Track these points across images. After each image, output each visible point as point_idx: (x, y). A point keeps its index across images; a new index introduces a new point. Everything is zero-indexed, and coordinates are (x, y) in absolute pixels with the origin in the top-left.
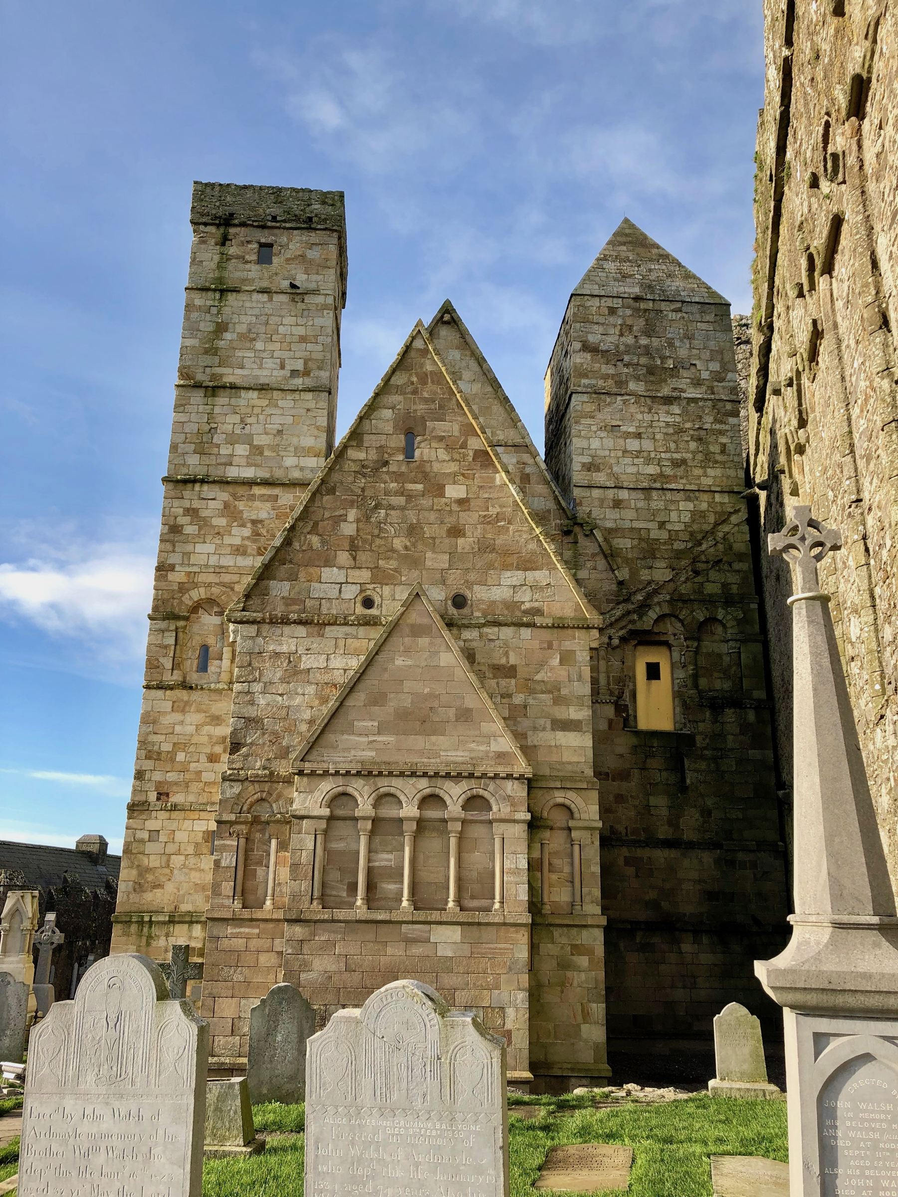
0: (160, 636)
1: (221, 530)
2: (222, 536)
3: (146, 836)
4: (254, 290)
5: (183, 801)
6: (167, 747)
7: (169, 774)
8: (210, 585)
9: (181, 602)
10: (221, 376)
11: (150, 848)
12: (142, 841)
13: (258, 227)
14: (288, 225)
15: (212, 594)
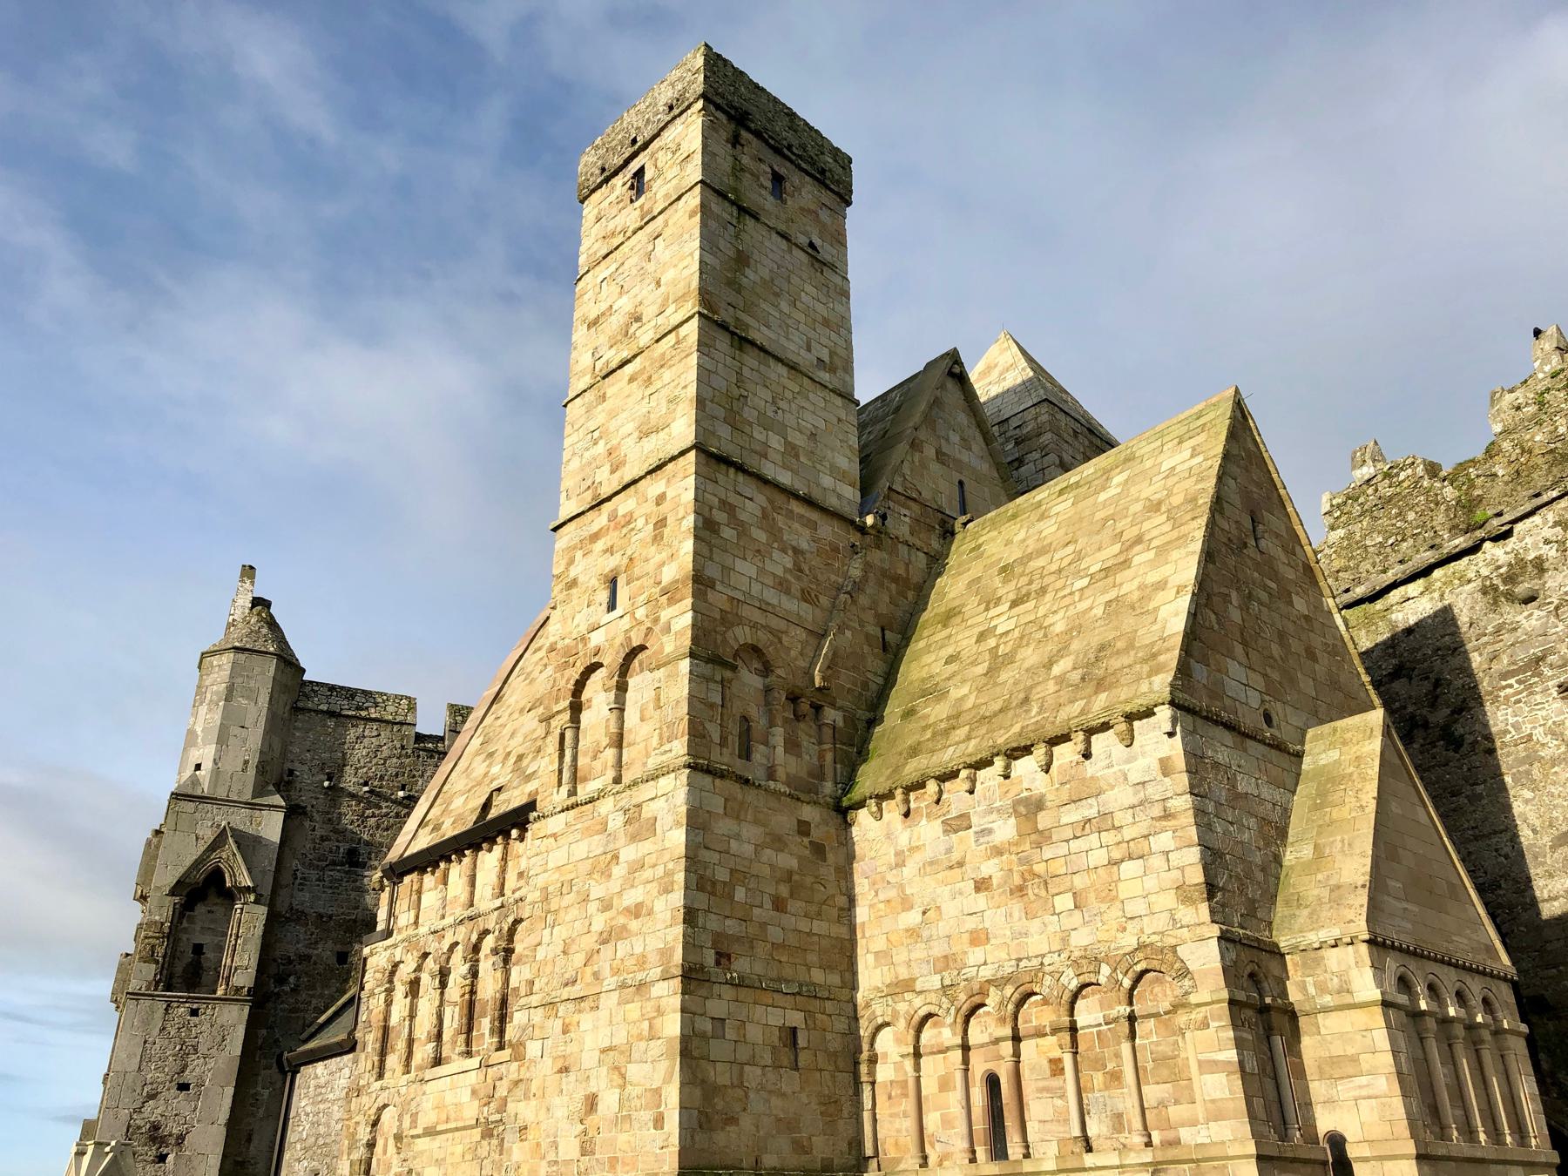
0: (704, 686)
1: (762, 548)
2: (764, 557)
4: (773, 228)
5: (748, 971)
6: (722, 875)
7: (728, 922)
9: (725, 640)
10: (747, 326)
11: (717, 1049)
12: (703, 1036)
13: (771, 147)
14: (804, 165)
15: (758, 640)
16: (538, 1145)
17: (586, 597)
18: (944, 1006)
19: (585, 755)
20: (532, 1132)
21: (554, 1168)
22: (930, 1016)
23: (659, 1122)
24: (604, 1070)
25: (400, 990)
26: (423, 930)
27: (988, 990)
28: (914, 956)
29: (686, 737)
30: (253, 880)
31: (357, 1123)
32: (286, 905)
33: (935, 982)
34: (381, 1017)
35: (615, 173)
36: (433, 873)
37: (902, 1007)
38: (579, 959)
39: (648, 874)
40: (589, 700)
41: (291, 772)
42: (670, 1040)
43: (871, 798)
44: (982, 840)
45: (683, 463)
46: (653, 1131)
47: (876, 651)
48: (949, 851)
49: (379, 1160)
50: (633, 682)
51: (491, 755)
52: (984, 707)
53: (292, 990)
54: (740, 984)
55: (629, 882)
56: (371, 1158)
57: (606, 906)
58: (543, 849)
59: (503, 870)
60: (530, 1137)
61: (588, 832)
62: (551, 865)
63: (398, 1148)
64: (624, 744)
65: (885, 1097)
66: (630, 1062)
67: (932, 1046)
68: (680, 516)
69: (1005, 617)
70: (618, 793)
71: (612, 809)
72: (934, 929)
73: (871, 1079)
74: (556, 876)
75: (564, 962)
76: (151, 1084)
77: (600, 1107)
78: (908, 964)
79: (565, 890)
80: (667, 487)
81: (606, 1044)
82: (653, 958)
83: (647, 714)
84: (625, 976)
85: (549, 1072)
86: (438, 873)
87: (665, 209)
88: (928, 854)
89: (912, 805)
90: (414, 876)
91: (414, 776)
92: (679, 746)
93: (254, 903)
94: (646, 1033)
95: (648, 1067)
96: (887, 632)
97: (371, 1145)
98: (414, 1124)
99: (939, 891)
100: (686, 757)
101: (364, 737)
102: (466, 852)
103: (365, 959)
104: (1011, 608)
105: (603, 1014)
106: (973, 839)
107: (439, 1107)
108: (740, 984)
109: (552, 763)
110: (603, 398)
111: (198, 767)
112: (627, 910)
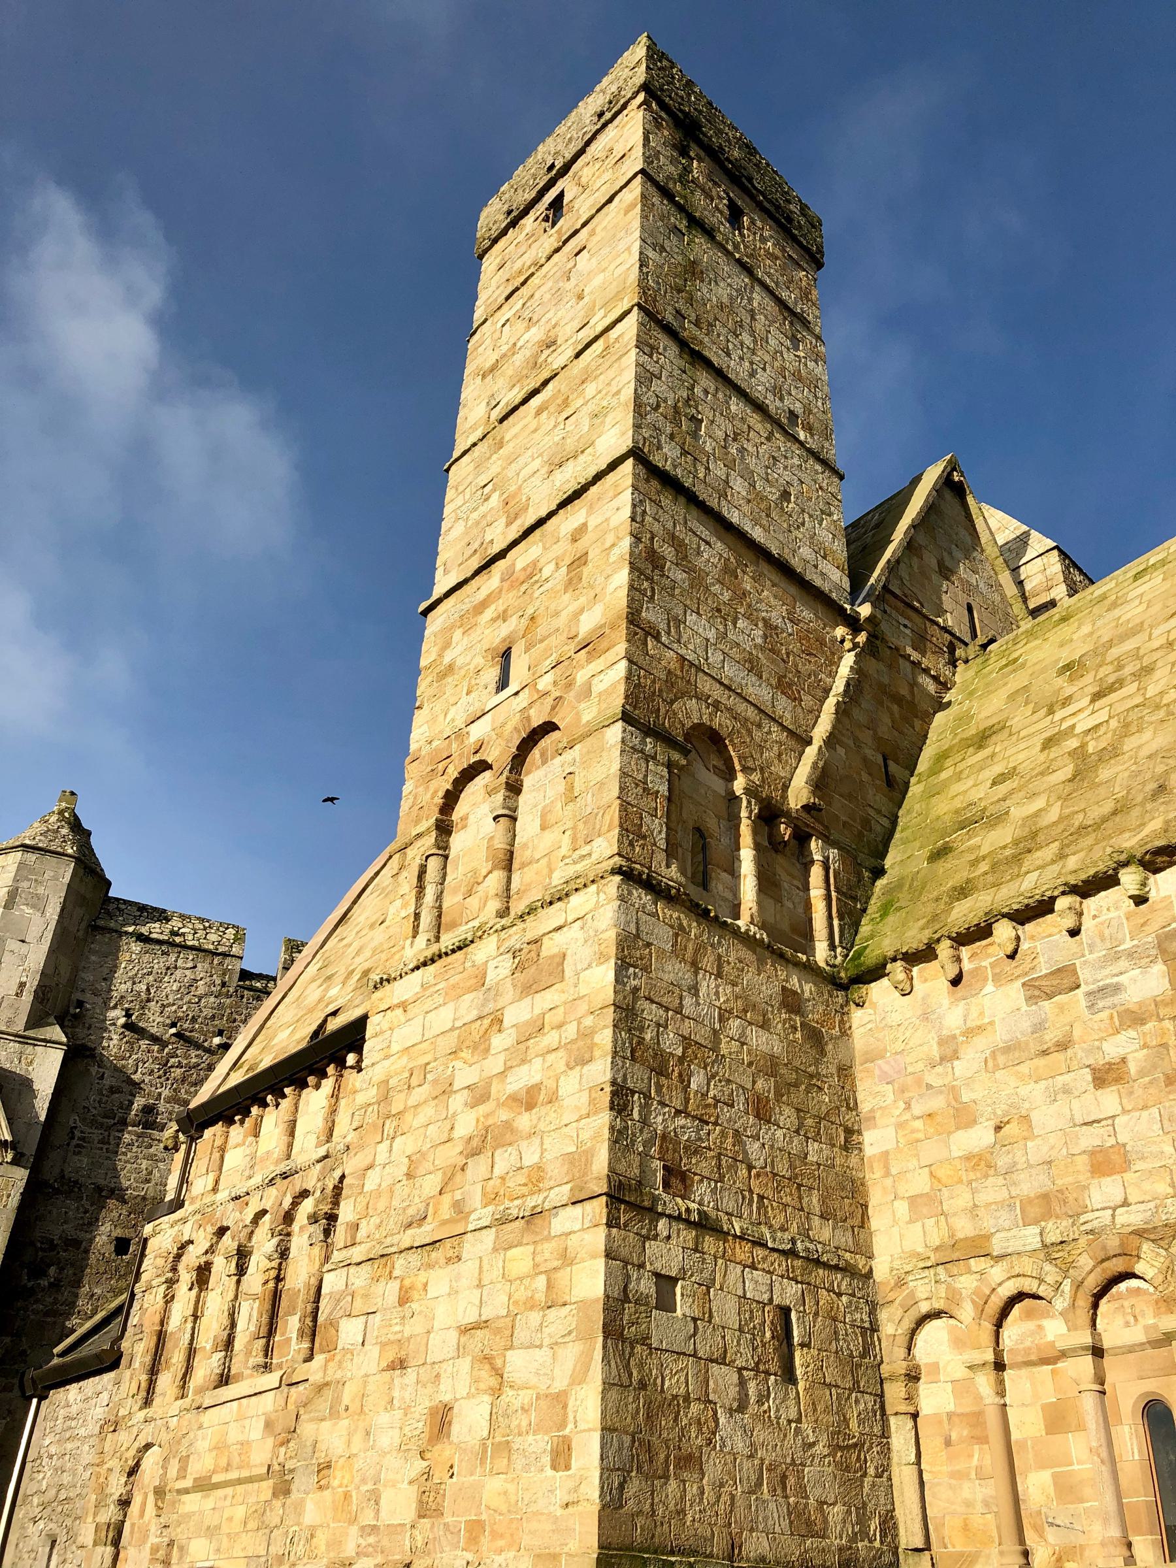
3: (646, 1286)
6: (671, 1043)
8: (716, 705)
16: (347, 1496)
17: (465, 684)
18: (1050, 1279)
19: (455, 891)
20: (338, 1474)
21: (371, 1540)
22: (1020, 1297)
23: (561, 1456)
24: (465, 1364)
25: (186, 1277)
26: (223, 1195)
27: (1139, 1248)
28: (983, 1197)
29: (617, 830)
30: (12, 1132)
31: (111, 1470)
32: (57, 1171)
33: (1030, 1237)
34: (157, 1319)
35: (525, 212)
36: (242, 1122)
37: (966, 1283)
38: (430, 1184)
39: (551, 1038)
40: (465, 818)
41: (80, 1004)
42: (583, 1304)
43: (894, 960)
44: (1101, 1004)
45: (614, 479)
46: (549, 1472)
47: (878, 782)
48: (1039, 1027)
49: (133, 1525)
50: (528, 781)
51: (329, 978)
52: (1081, 816)
53: (51, 1285)
54: (704, 1225)
55: (520, 1053)
56: (123, 1522)
57: (479, 1095)
58: (385, 1026)
59: (333, 1111)
60: (335, 1483)
61: (455, 994)
62: (395, 1048)
63: (159, 1508)
64: (515, 866)
65: (939, 1441)
66: (511, 1347)
67: (1027, 1351)
68: (608, 545)
69: (1087, 712)
70: (504, 929)
71: (494, 954)
72: (1019, 1153)
73: (911, 1410)
74: (405, 1059)
75: (407, 1190)
77: (455, 1429)
78: (973, 1211)
79: (414, 1081)
80: (589, 514)
81: (471, 1317)
82: (556, 1171)
83: (551, 818)
84: (507, 1204)
85: (373, 1368)
86: (249, 1122)
87: (592, 217)
88: (1000, 1035)
89: (967, 966)
90: (218, 1128)
91: (235, 1020)
92: (605, 844)
93: (12, 1163)
94: (540, 1296)
95: (543, 1355)
96: (891, 763)
97: (125, 1503)
98: (182, 1474)
99: (1023, 1091)
100: (617, 858)
101: (176, 967)
102: (287, 1090)
103: (146, 1240)
104: (1093, 701)
105: (468, 1268)
106: (1083, 1003)
107: (219, 1447)
108: (704, 1225)
109: (404, 906)
110: (500, 445)
112: (514, 1098)
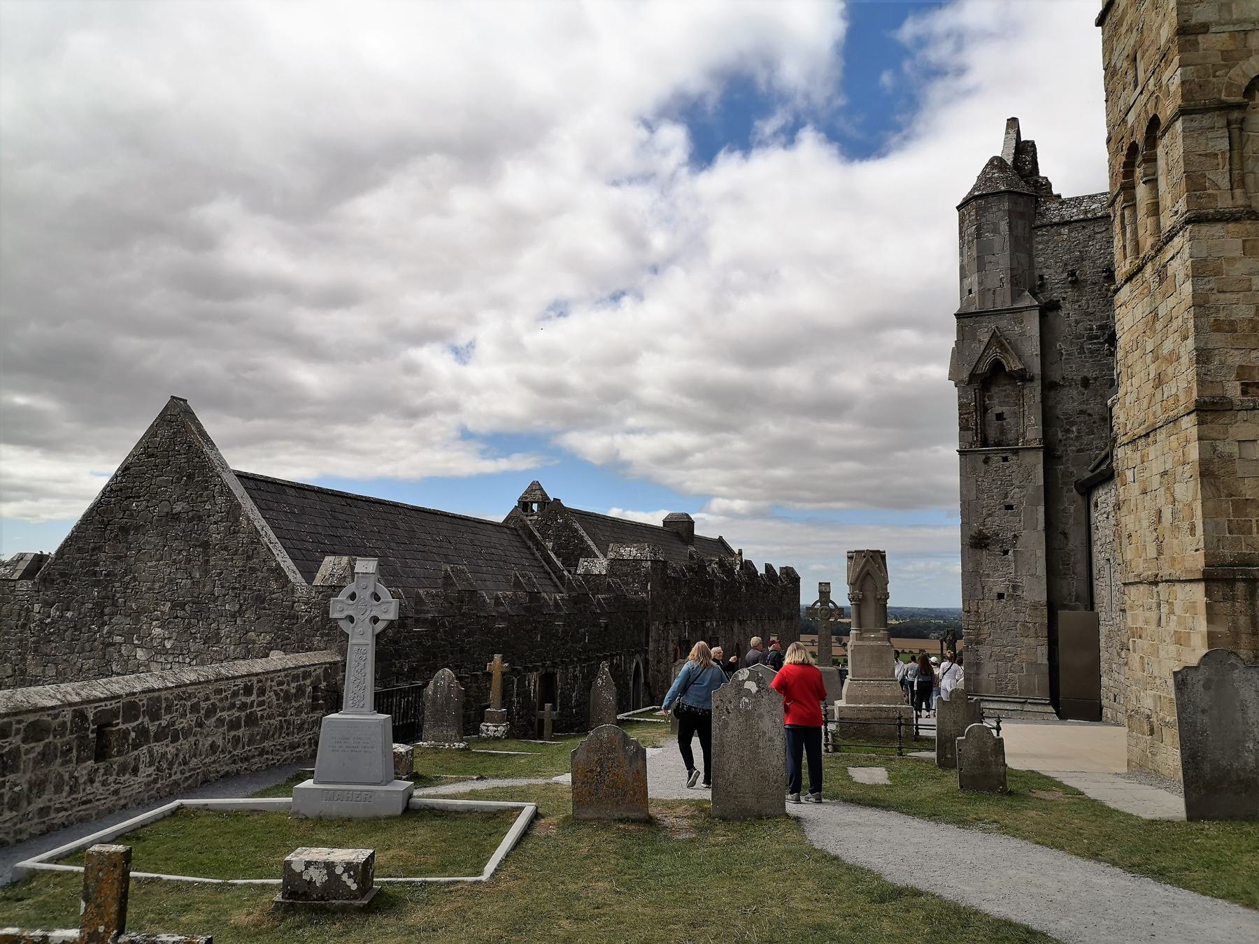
41: (1041, 277)
53: (1077, 437)
76: (987, 507)
103: (1111, 409)
111: (970, 291)
